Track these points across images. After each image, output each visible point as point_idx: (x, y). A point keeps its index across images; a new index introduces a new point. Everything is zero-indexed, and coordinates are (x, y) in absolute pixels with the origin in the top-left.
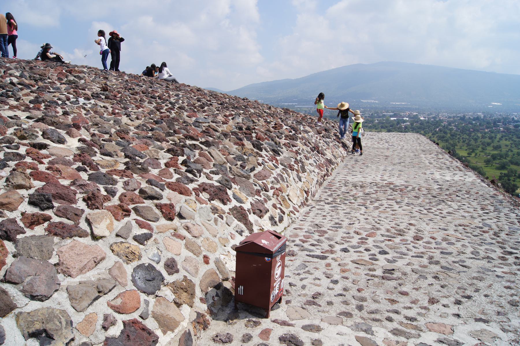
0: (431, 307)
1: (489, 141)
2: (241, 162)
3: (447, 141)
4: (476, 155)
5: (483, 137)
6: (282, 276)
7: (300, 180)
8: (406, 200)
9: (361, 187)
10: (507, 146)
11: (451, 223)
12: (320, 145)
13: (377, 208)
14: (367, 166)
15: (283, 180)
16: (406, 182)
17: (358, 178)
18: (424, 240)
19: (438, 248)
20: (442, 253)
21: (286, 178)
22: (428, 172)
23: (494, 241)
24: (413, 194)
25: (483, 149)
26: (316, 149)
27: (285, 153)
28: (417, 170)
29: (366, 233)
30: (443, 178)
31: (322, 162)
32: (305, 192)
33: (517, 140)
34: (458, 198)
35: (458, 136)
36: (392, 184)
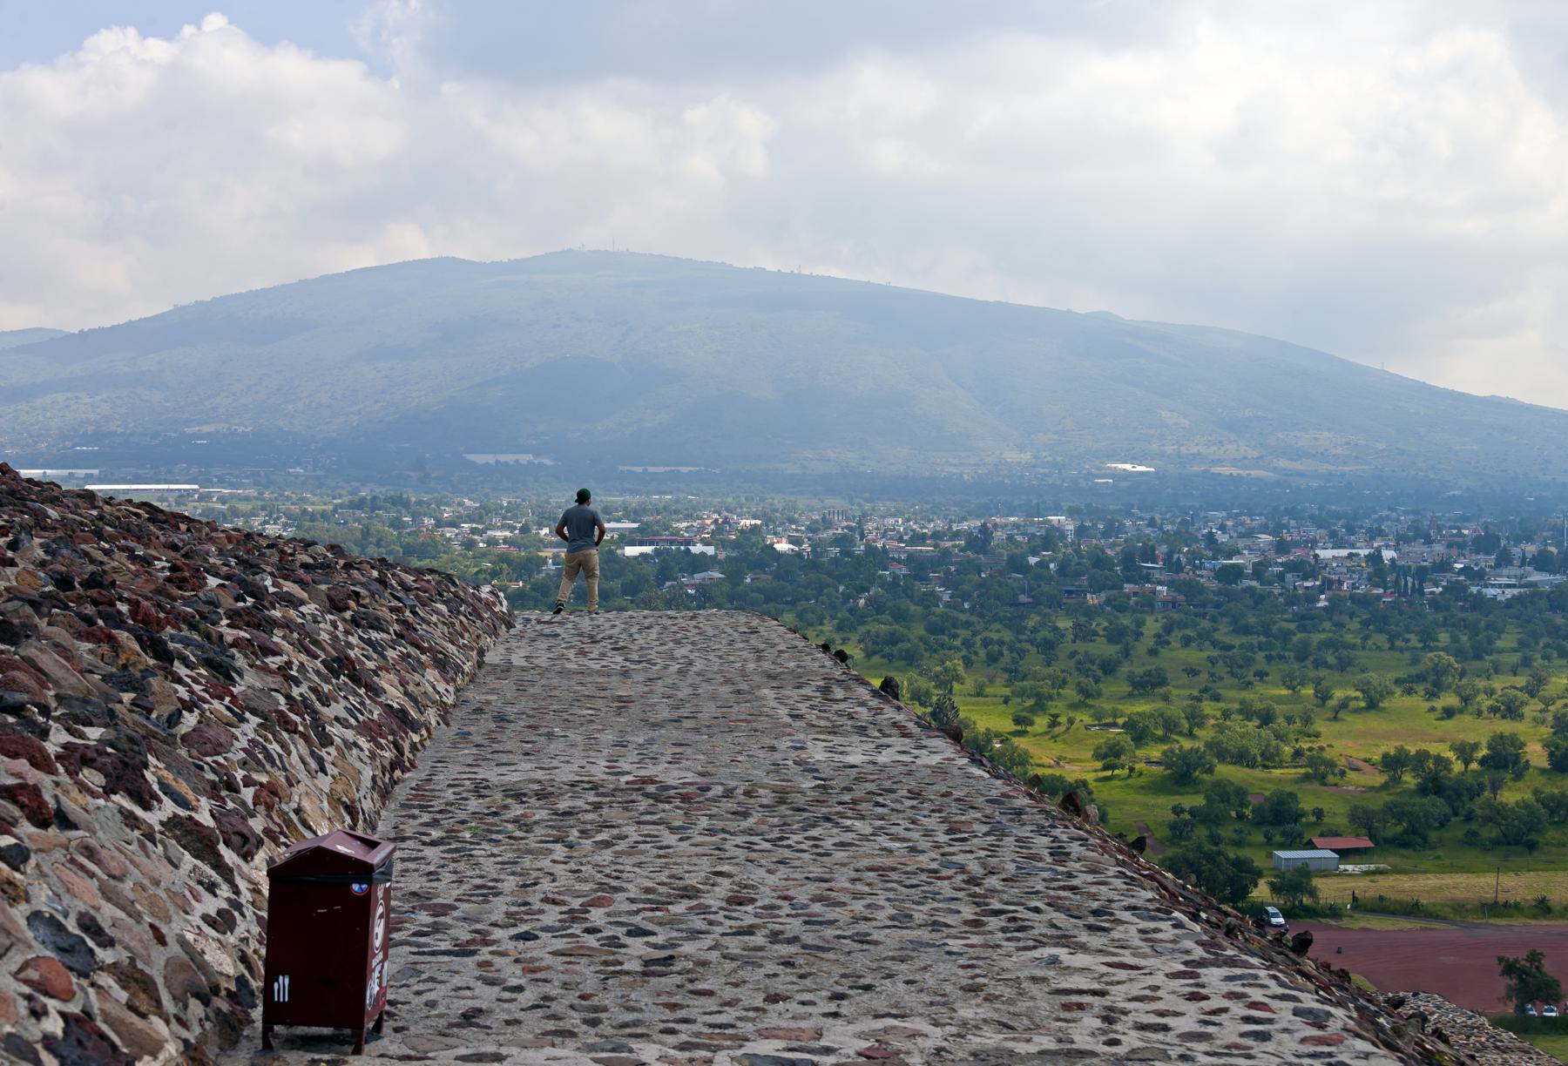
0: (770, 1007)
1: (1111, 651)
2: (133, 695)
4: (1054, 723)
6: (388, 944)
7: (323, 770)
8: (704, 822)
9: (541, 796)
10: (1192, 672)
11: (843, 865)
12: (352, 654)
13: (606, 844)
14: (550, 736)
15: (273, 764)
16: (702, 775)
17: (522, 772)
18: (759, 904)
19: (797, 915)
20: (806, 923)
21: (280, 756)
22: (784, 744)
23: (960, 895)
24: (730, 805)
25: (1085, 692)
26: (340, 665)
27: (247, 682)
28: (742, 740)
29: (580, 901)
30: (837, 757)
31: (375, 717)
32: (346, 807)
33: (1237, 641)
34: (880, 810)
35: (964, 633)
36: (653, 782)
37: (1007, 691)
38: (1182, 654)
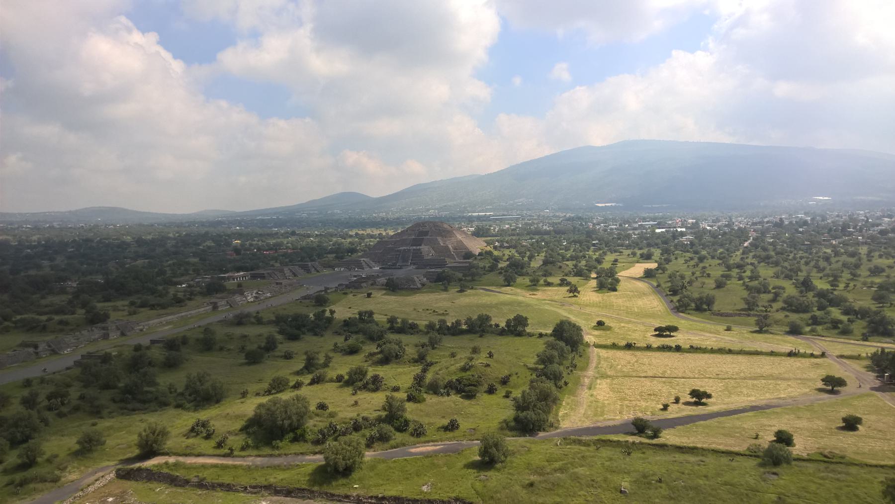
1: (852, 260)
3: (777, 264)
4: (847, 286)
5: (837, 254)
25: (854, 275)
35: (792, 256)
37: (820, 275)
38: (880, 261)
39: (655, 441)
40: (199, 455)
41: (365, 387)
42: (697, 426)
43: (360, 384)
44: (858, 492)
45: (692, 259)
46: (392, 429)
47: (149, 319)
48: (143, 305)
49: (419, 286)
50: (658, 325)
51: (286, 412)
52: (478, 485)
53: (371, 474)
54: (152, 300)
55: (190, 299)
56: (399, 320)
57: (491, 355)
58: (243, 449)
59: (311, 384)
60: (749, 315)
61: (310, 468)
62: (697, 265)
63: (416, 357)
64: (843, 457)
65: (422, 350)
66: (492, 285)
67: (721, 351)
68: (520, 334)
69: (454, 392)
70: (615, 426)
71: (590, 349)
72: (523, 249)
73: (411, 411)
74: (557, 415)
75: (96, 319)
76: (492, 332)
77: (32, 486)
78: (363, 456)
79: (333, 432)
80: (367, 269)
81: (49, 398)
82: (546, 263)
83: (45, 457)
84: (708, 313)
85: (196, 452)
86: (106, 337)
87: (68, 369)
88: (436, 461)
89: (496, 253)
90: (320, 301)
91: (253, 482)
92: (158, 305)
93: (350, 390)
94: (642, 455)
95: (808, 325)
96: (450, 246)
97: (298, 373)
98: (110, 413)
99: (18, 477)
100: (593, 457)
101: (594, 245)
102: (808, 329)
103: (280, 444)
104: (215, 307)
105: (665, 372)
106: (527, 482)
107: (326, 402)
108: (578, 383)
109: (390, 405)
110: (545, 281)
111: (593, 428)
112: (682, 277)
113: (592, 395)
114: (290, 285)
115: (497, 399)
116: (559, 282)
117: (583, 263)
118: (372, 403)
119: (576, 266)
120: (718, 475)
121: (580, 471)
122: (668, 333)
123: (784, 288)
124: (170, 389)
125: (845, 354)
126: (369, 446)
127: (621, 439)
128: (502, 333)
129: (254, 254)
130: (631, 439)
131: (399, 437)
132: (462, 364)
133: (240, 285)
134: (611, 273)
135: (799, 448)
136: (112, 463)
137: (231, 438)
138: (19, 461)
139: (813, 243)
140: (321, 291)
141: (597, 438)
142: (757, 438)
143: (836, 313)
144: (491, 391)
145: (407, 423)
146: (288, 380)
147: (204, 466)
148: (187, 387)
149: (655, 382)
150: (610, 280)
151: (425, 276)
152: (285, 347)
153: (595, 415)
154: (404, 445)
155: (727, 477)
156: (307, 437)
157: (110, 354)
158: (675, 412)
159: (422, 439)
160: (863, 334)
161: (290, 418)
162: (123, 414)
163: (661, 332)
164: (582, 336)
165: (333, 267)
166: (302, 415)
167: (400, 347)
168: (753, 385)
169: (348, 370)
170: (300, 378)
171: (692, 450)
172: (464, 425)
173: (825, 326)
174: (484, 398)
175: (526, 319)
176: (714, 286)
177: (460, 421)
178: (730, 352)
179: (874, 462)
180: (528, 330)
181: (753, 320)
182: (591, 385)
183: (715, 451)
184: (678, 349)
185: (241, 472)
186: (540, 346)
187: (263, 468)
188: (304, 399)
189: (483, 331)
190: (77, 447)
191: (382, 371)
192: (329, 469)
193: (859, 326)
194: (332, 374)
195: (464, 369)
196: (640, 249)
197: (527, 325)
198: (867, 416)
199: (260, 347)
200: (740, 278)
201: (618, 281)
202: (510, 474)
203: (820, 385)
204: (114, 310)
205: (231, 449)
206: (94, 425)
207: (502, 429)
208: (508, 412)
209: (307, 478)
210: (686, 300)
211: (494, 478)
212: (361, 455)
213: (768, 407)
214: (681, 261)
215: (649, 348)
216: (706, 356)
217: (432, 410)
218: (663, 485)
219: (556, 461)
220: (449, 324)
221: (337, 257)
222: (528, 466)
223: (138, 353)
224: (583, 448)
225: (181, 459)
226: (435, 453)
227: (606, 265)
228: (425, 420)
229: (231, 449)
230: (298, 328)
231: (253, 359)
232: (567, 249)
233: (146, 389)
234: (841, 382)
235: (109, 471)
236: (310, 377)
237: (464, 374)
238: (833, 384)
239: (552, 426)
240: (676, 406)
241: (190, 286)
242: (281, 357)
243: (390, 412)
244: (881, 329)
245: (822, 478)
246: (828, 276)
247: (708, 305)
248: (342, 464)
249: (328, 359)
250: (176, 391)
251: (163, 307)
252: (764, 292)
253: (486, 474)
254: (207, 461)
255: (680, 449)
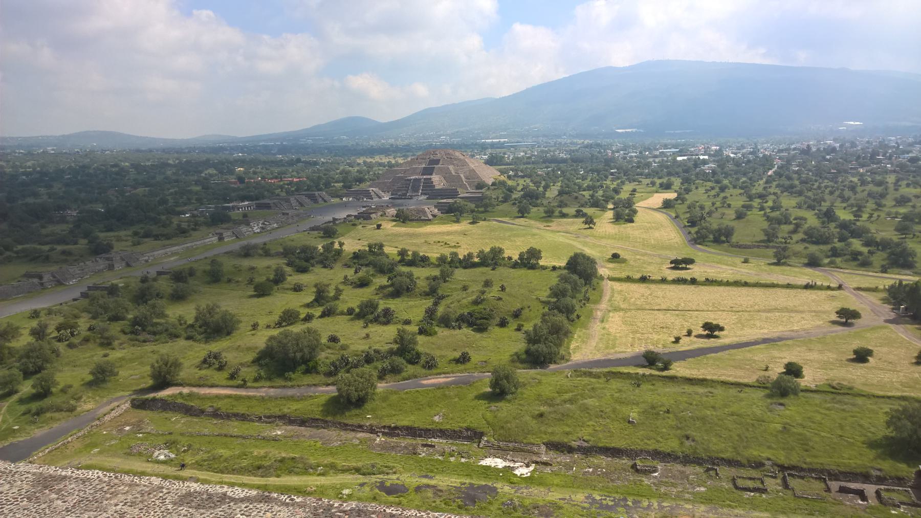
1: (879, 189)
3: (800, 193)
4: (871, 216)
5: (863, 183)
25: (879, 206)
35: (816, 184)
37: (844, 205)
39: (665, 373)
40: (212, 386)
41: (376, 320)
42: (707, 358)
43: (371, 317)
44: (862, 422)
45: (713, 188)
46: (404, 362)
47: (153, 250)
48: (147, 235)
49: (431, 217)
50: (674, 258)
51: (298, 345)
52: (488, 415)
53: (384, 405)
54: (155, 229)
55: (194, 230)
56: (410, 253)
57: (503, 288)
58: (256, 380)
59: (321, 317)
60: (767, 247)
61: (323, 399)
62: (718, 195)
63: (427, 290)
64: (850, 388)
65: (433, 283)
66: (506, 216)
67: (737, 284)
68: (533, 267)
69: (466, 325)
70: (626, 359)
71: (604, 283)
72: (538, 179)
73: (422, 344)
74: (568, 348)
75: (99, 250)
76: (505, 265)
77: (48, 415)
78: (375, 388)
79: (345, 364)
80: (376, 199)
81: (58, 329)
82: (561, 193)
83: (60, 387)
84: (725, 245)
85: (209, 383)
86: (111, 268)
87: (75, 300)
88: (447, 393)
89: (510, 183)
90: (329, 232)
91: (267, 412)
92: (163, 235)
93: (361, 323)
94: (652, 387)
95: (828, 257)
96: (462, 176)
97: (308, 306)
98: (121, 344)
99: (34, 406)
100: (603, 388)
101: (612, 174)
102: (826, 261)
103: (293, 376)
104: (221, 239)
105: (679, 305)
106: (537, 412)
107: (337, 334)
108: (590, 316)
109: (402, 338)
110: (561, 212)
111: (604, 360)
112: (702, 208)
113: (604, 328)
114: (298, 215)
115: (509, 331)
116: (574, 213)
117: (600, 193)
118: (383, 336)
119: (592, 196)
120: (726, 406)
121: (590, 402)
122: (684, 266)
123: (805, 219)
124: (179, 321)
125: (862, 286)
126: (381, 378)
127: (632, 372)
128: (515, 266)
129: (258, 183)
130: (641, 371)
131: (410, 369)
132: (474, 297)
133: (245, 216)
134: (629, 204)
135: (809, 379)
136: (127, 393)
137: (244, 370)
138: (34, 391)
139: (839, 172)
140: (329, 222)
141: (607, 370)
142: (766, 369)
143: (856, 244)
144: (503, 324)
145: (418, 355)
146: (298, 312)
147: (218, 397)
148: (197, 319)
149: (668, 315)
150: (627, 211)
151: (435, 207)
152: (294, 278)
153: (607, 348)
154: (416, 377)
155: (735, 408)
156: (319, 369)
157: (117, 285)
158: (686, 344)
159: (434, 371)
160: (883, 266)
161: (301, 350)
162: (134, 345)
163: (677, 264)
164: (596, 269)
165: (341, 197)
166: (314, 348)
167: (412, 280)
168: (767, 318)
169: (358, 303)
170: (311, 311)
171: (702, 382)
172: (475, 357)
173: (845, 258)
174: (496, 331)
175: (540, 252)
176: (734, 217)
177: (471, 353)
178: (746, 284)
179: (881, 393)
180: (542, 262)
181: (771, 252)
182: (603, 318)
183: (724, 383)
184: (693, 281)
185: (254, 402)
186: (554, 279)
187: (276, 398)
188: (315, 332)
189: (496, 264)
190: (91, 378)
191: (393, 304)
192: (342, 400)
193: (879, 258)
194: (343, 307)
195: (476, 303)
196: (660, 178)
197: (540, 258)
198: (879, 348)
199: (268, 280)
200: (762, 209)
201: (635, 212)
202: (520, 405)
203: (834, 317)
204: (118, 241)
205: (244, 380)
206: (105, 356)
207: (513, 361)
208: (520, 346)
209: (321, 409)
210: (705, 232)
211: (504, 409)
212: (373, 387)
213: (780, 339)
214: (701, 190)
215: (664, 281)
216: (722, 288)
217: (443, 343)
218: (671, 415)
219: (566, 393)
220: (461, 257)
221: (344, 187)
222: (539, 397)
223: (146, 285)
224: (593, 380)
225: (195, 390)
226: (447, 385)
227: (624, 195)
228: (437, 353)
229: (244, 380)
230: (307, 260)
231: (262, 291)
232: (584, 178)
233: (155, 320)
234: (855, 315)
235: (123, 401)
236: (321, 309)
237: (475, 307)
238: (847, 317)
239: (563, 358)
240: (688, 339)
241: (193, 216)
242: (291, 289)
243: (402, 345)
244: (901, 261)
245: (828, 409)
246: (852, 206)
247: (727, 237)
248: (354, 396)
249: (339, 292)
250: (185, 323)
251: (168, 237)
252: (785, 223)
253: (497, 404)
254: (220, 391)
255: (690, 381)
